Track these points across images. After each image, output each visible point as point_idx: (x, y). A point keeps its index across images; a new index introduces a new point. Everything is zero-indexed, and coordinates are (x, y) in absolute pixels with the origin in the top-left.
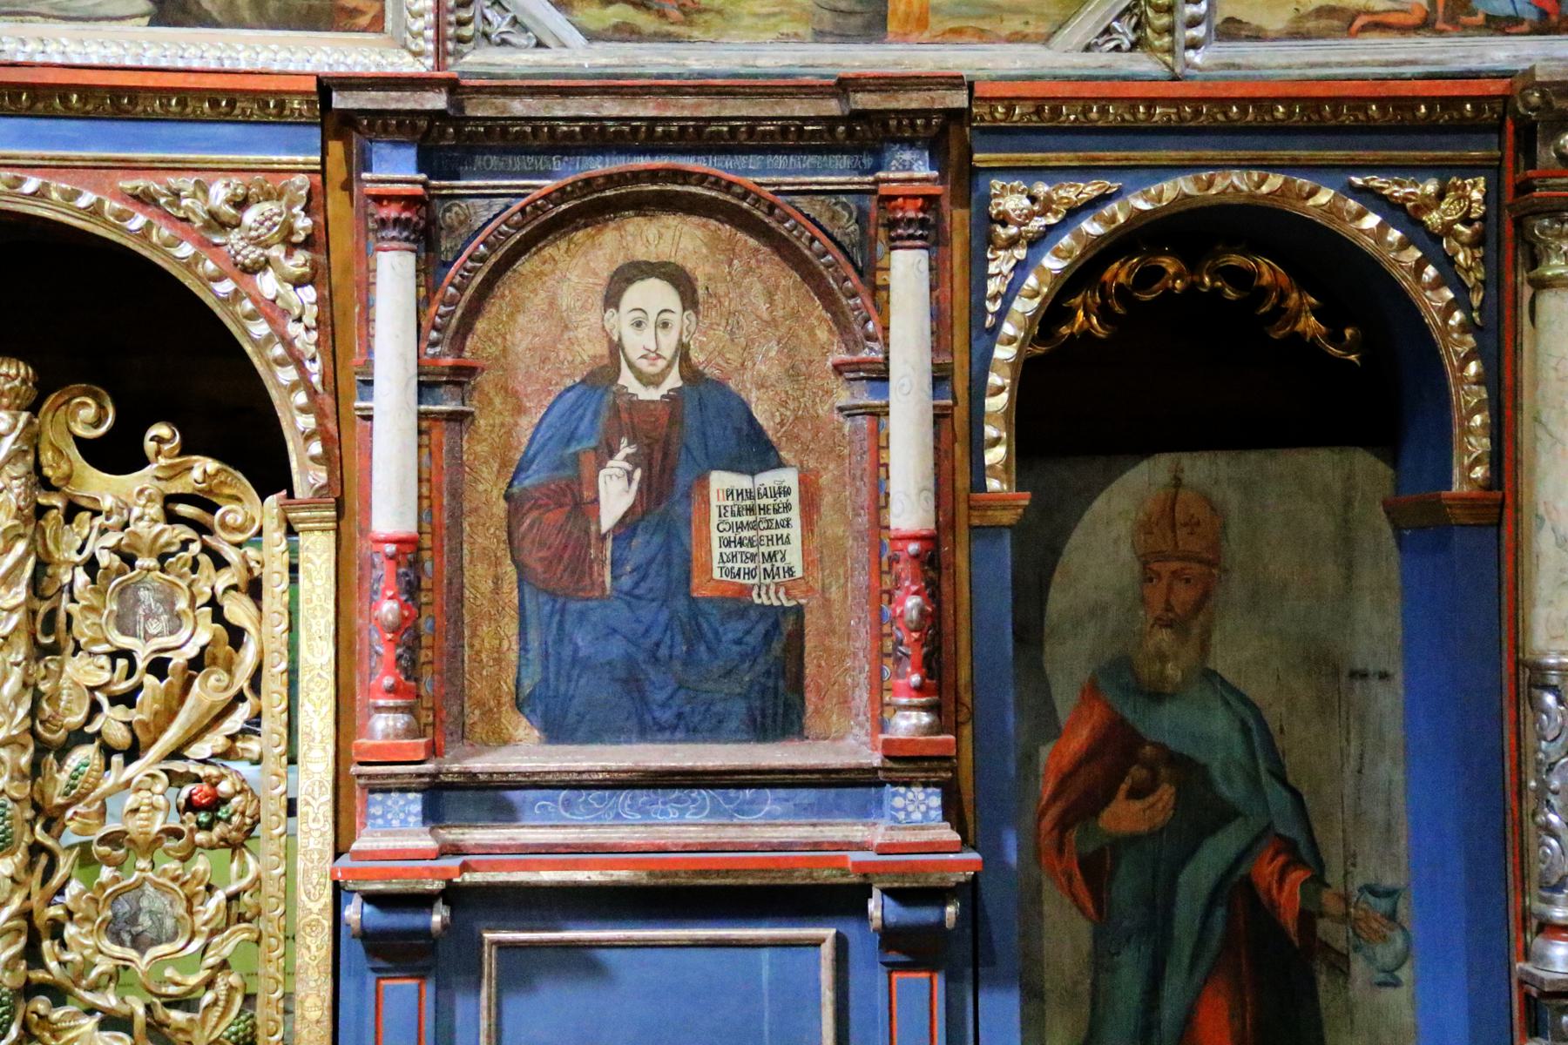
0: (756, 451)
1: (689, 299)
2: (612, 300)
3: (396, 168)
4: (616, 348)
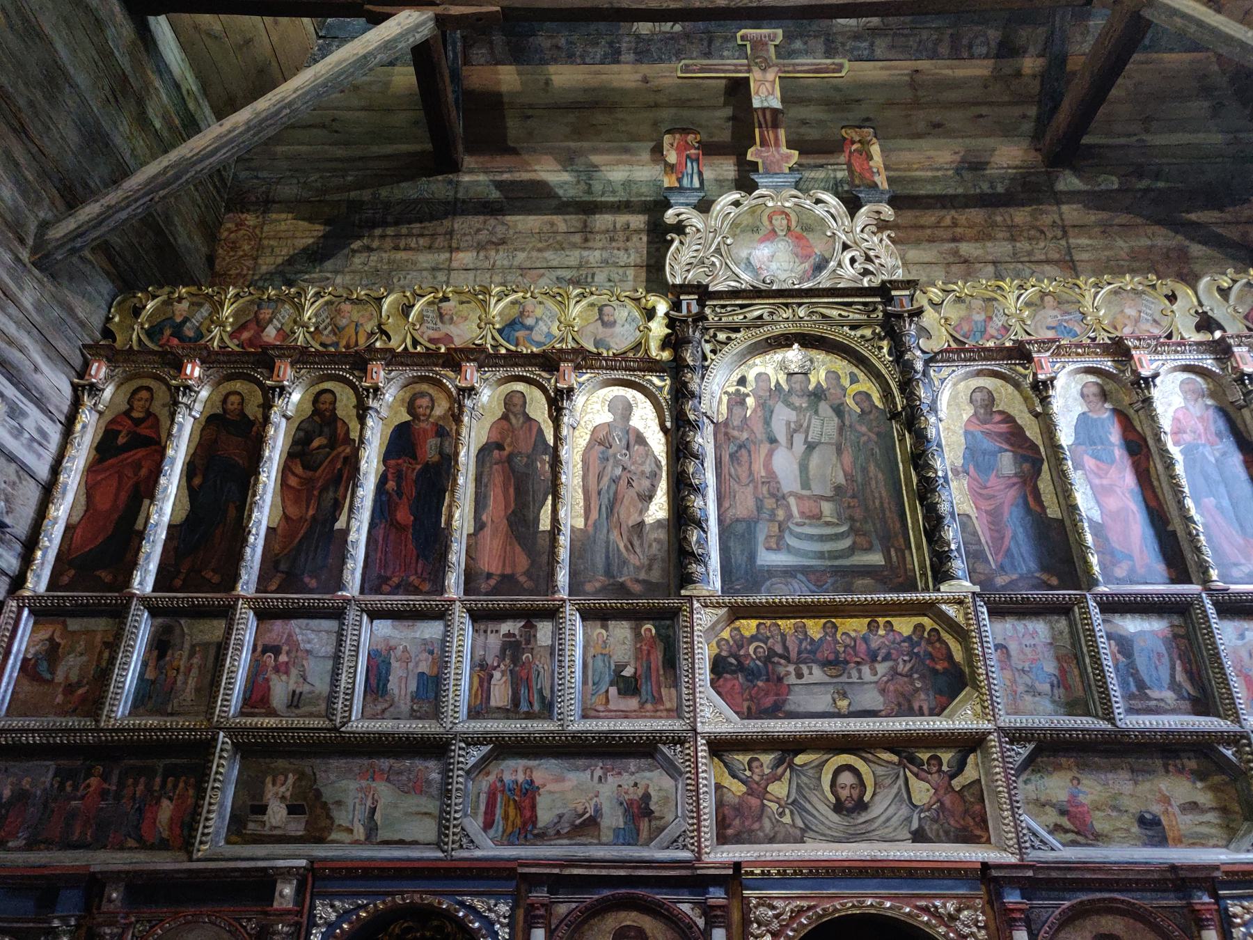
3: (1013, 898)
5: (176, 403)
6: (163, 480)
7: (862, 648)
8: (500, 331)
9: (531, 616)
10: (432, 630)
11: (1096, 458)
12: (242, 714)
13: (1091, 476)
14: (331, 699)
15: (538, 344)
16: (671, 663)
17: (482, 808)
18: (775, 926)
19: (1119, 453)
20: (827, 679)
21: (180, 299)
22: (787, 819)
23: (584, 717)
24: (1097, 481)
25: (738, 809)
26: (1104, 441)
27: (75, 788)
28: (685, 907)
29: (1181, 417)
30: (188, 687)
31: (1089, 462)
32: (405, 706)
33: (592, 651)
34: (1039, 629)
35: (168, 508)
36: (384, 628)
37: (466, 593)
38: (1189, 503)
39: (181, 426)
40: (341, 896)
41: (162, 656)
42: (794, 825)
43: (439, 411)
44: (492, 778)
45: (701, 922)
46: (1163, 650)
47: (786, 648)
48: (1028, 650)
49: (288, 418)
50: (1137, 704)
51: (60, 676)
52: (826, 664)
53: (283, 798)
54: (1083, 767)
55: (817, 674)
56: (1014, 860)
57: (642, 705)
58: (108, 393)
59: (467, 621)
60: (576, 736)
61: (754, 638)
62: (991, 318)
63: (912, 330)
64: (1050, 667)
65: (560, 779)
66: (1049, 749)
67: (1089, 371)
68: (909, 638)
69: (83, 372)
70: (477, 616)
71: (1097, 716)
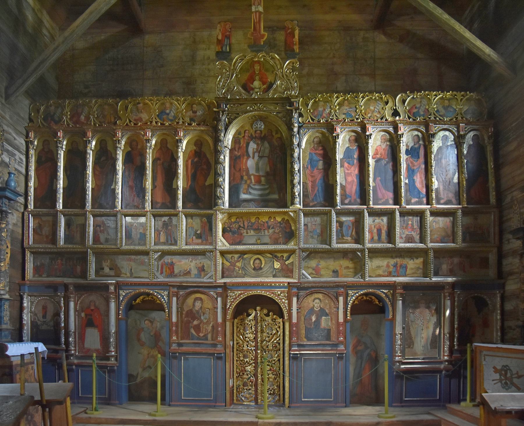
0: (327, 315)
1: (321, 302)
2: (314, 301)
3: (295, 290)
4: (314, 306)
5: (57, 147)
6: (58, 174)
7: (266, 225)
8: (158, 116)
9: (170, 215)
10: (142, 220)
11: (349, 163)
12: (93, 244)
13: (345, 170)
14: (116, 240)
15: (171, 120)
16: (211, 229)
17: (160, 269)
18: (234, 297)
19: (355, 161)
20: (255, 234)
21: (51, 106)
22: (240, 272)
23: (186, 245)
24: (347, 171)
25: (228, 270)
26: (351, 157)
27: (55, 263)
28: (212, 293)
29: (378, 149)
30: (78, 237)
31: (346, 165)
32: (137, 242)
33: (188, 226)
34: (318, 219)
35: (61, 182)
36: (128, 219)
37: (152, 208)
38: (371, 180)
39: (60, 154)
40: (126, 290)
41: (69, 228)
42: (242, 273)
43: (139, 147)
44: (162, 261)
45: (216, 296)
46: (351, 226)
47: (244, 225)
48: (313, 226)
49: (93, 151)
50: (340, 241)
51: (44, 233)
52: (255, 230)
53: (108, 266)
54: (321, 258)
55: (252, 232)
56: (296, 281)
57: (202, 241)
58: (36, 143)
59: (152, 217)
60: (183, 250)
61: (235, 222)
62: (325, 110)
63: (296, 116)
64: (319, 231)
65: (180, 262)
66: (312, 254)
67: (353, 131)
68: (280, 222)
69: (27, 136)
70: (155, 216)
71: (327, 245)
